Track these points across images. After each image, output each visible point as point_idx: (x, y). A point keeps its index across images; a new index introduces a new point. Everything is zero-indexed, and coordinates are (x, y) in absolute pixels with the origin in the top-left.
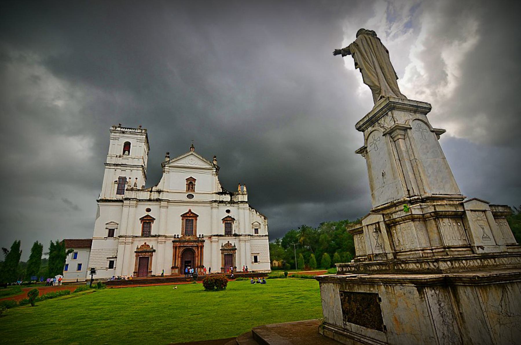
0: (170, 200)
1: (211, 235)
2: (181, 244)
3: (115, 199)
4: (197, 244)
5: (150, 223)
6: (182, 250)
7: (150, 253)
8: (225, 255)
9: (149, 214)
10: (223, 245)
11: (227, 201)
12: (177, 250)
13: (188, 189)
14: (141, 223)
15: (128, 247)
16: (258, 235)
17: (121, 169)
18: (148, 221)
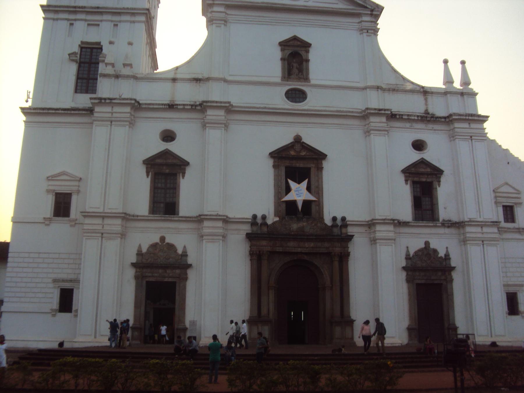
0: (234, 105)
7: (178, 271)
8: (418, 285)
10: (412, 253)
14: (148, 177)
17: (86, 20)
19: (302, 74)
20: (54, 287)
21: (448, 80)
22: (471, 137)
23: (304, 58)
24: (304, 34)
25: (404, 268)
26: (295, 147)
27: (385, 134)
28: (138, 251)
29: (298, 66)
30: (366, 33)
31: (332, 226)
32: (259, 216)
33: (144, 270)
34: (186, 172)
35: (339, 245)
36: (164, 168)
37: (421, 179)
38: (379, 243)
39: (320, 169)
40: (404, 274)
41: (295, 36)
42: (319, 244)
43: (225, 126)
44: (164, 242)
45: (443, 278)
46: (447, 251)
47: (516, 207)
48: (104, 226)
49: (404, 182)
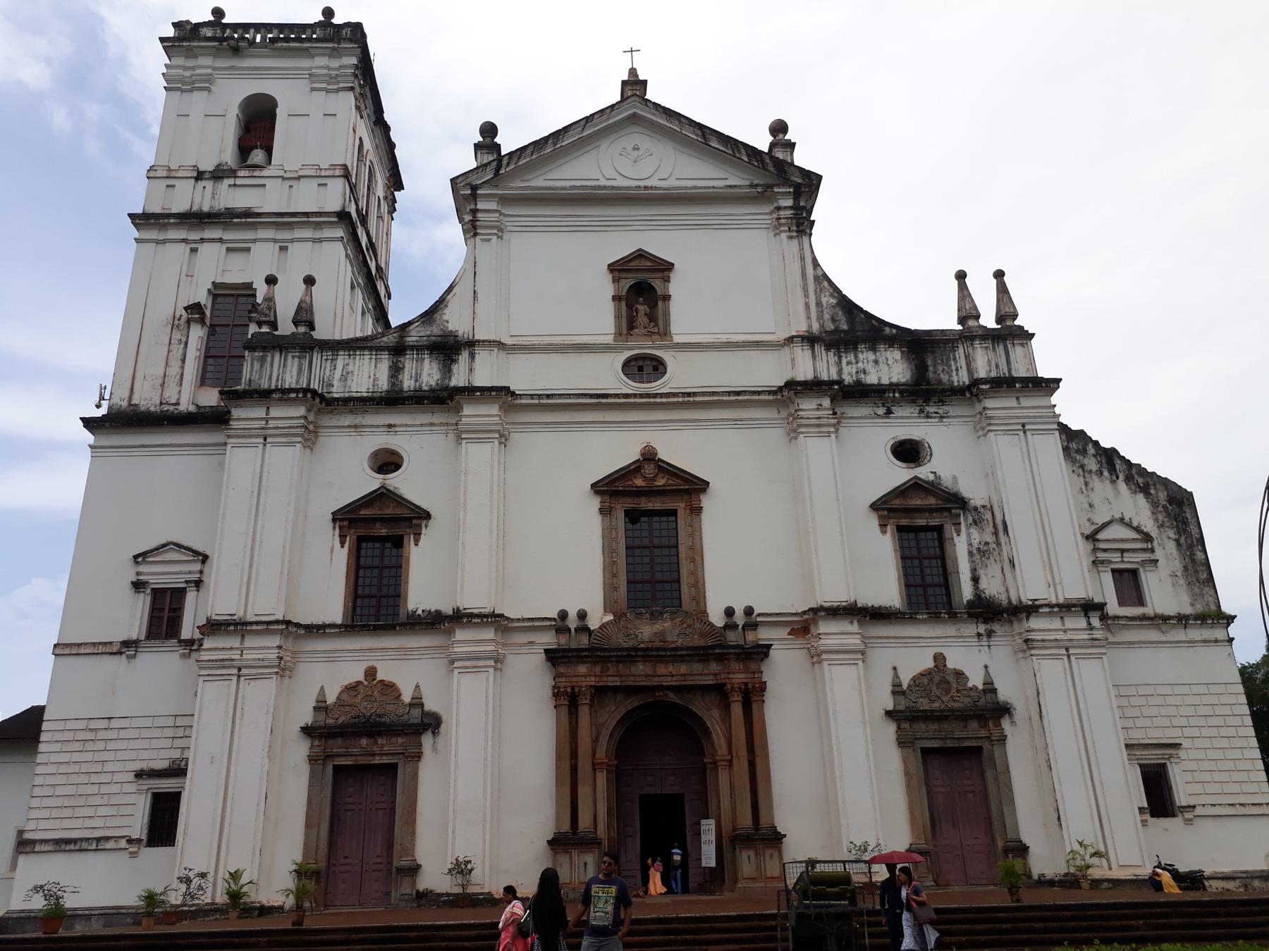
0: (517, 392)
1: (814, 611)
2: (604, 672)
3: (186, 406)
4: (716, 675)
5: (402, 537)
6: (613, 713)
8: (926, 752)
10: (905, 681)
11: (893, 387)
12: (584, 712)
13: (624, 325)
14: (342, 547)
15: (261, 693)
16: (1148, 610)
17: (221, 240)
18: (384, 532)
19: (657, 325)
20: (139, 792)
21: (968, 313)
22: (1023, 426)
23: (659, 293)
25: (889, 714)
26: (643, 471)
27: (829, 432)
29: (648, 311)
30: (785, 231)
31: (726, 627)
32: (572, 614)
33: (330, 742)
34: (424, 530)
35: (742, 667)
36: (378, 525)
37: (914, 521)
38: (827, 660)
39: (697, 511)
41: (640, 250)
42: (697, 667)
43: (501, 436)
45: (983, 733)
46: (987, 673)
47: (1145, 571)
48: (244, 652)
49: (877, 529)
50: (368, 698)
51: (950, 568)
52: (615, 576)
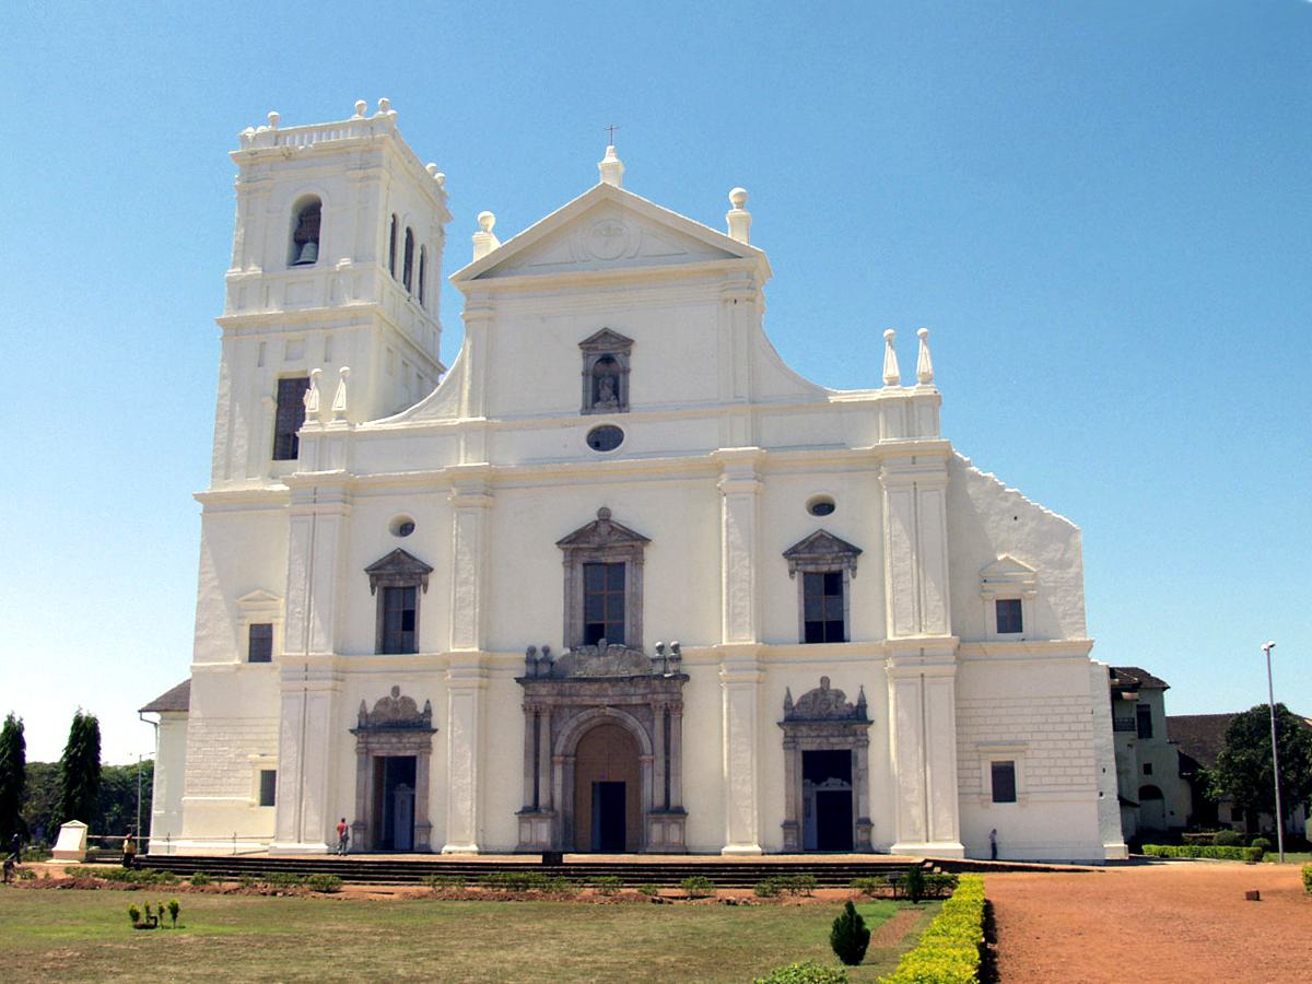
4: (644, 696)
5: (414, 588)
6: (567, 728)
9: (408, 544)
10: (795, 700)
12: (545, 721)
13: (590, 398)
14: (373, 593)
18: (401, 584)
19: (618, 398)
24: (620, 326)
28: (361, 712)
36: (398, 577)
39: (639, 562)
40: (781, 733)
44: (398, 694)
50: (396, 710)
51: (845, 608)
52: (572, 617)
